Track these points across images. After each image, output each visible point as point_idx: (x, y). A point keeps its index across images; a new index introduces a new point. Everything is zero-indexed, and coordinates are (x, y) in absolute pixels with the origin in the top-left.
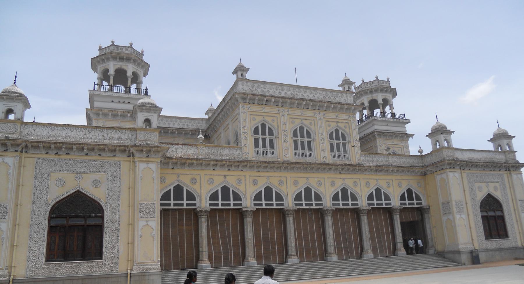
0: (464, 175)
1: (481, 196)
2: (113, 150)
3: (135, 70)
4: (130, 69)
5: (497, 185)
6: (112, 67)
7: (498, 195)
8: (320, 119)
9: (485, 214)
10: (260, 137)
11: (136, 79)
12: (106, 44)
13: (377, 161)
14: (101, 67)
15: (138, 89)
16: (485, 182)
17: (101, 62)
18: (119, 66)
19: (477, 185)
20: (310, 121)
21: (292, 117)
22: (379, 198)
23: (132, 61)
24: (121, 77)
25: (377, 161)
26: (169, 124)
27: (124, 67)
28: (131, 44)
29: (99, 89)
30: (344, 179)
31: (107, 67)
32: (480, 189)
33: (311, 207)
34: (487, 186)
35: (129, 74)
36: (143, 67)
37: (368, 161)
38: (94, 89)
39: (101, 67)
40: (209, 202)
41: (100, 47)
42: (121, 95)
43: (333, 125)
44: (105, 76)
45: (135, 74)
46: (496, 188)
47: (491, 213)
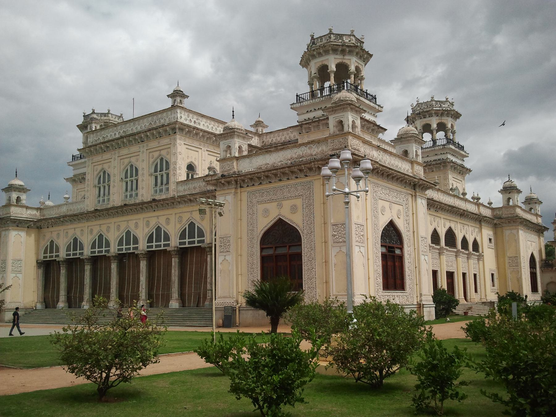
0: (245, 196)
1: (264, 223)
5: (299, 202)
7: (296, 220)
8: (143, 152)
9: (271, 252)
10: (101, 185)
13: (195, 188)
16: (276, 200)
19: (261, 207)
20: (136, 157)
21: (122, 157)
22: (191, 236)
25: (195, 188)
30: (158, 217)
32: (266, 212)
33: (129, 252)
34: (280, 206)
37: (184, 190)
40: (65, 253)
43: (156, 154)
46: (294, 209)
47: (281, 251)
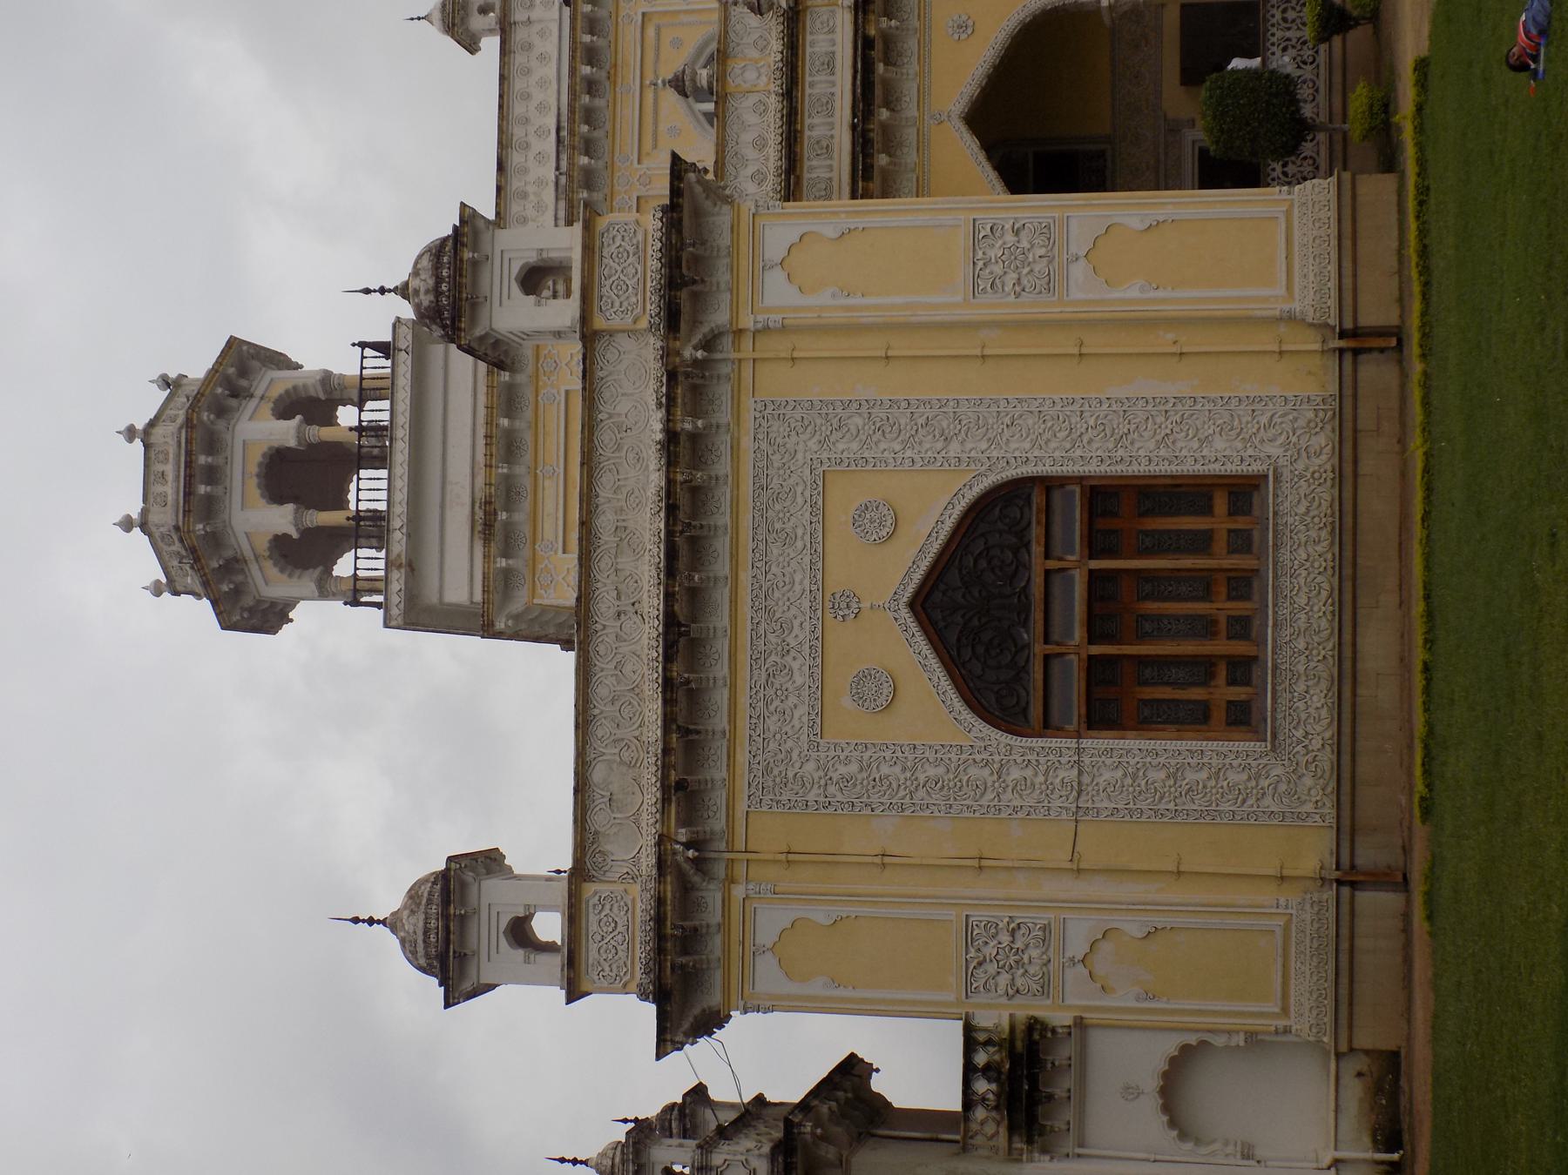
2: (687, 385)
3: (267, 408)
4: (261, 430)
6: (260, 519)
11: (315, 402)
12: (140, 560)
14: (270, 583)
15: (363, 392)
17: (240, 578)
18: (253, 482)
23: (221, 425)
24: (309, 474)
26: (541, 133)
27: (256, 457)
28: (130, 434)
29: (373, 586)
31: (263, 544)
35: (286, 432)
36: (244, 372)
38: (378, 605)
39: (270, 583)
41: (157, 590)
42: (401, 484)
44: (308, 554)
45: (287, 407)
